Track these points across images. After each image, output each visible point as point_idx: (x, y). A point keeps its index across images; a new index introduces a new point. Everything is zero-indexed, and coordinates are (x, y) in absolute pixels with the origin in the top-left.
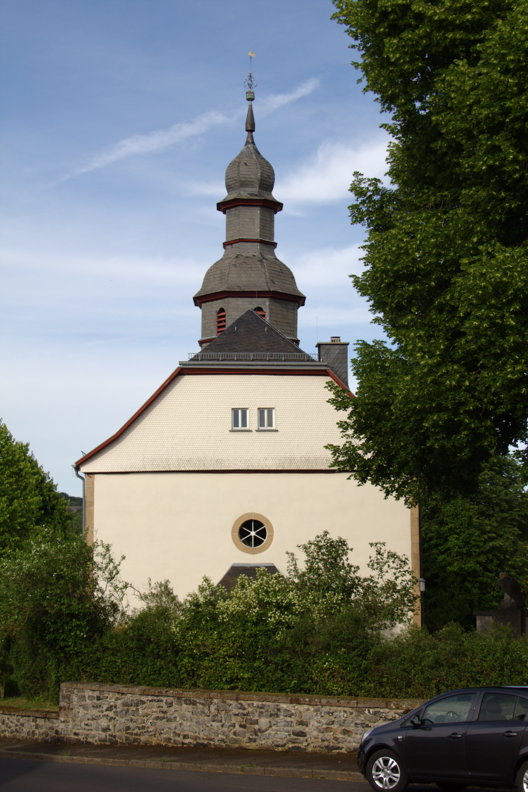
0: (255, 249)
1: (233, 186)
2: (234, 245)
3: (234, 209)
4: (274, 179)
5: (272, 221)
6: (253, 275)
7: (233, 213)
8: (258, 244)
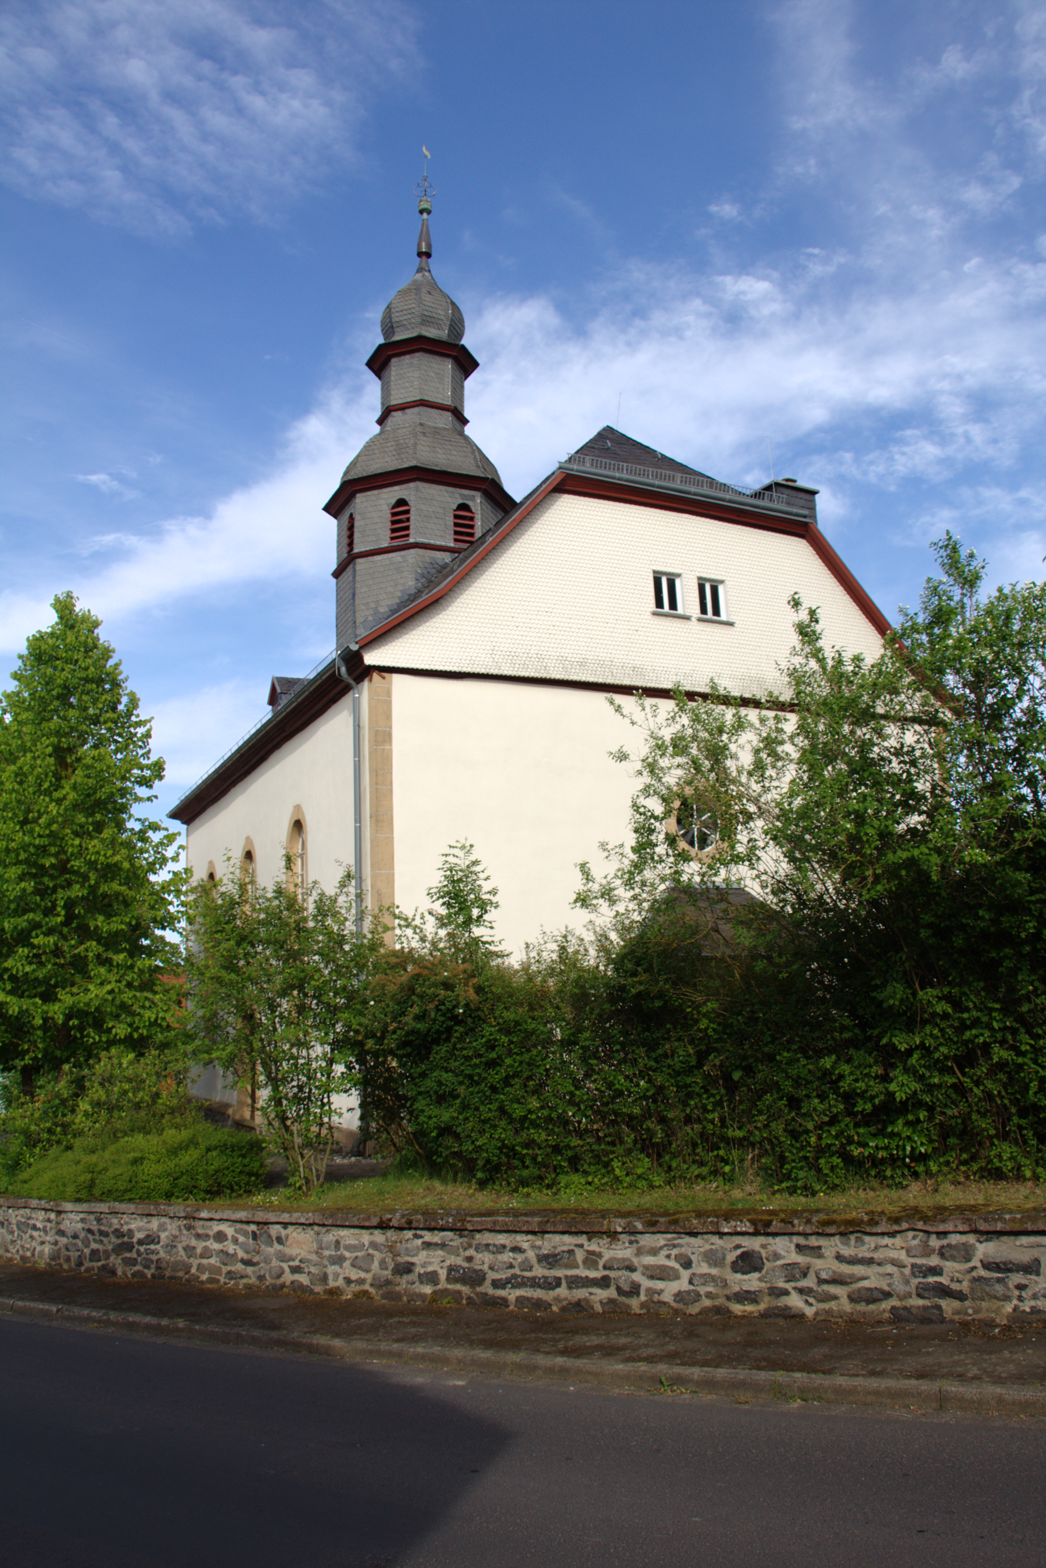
0: (446, 419)
1: (405, 323)
2: (407, 411)
3: (407, 357)
4: (464, 327)
5: (462, 387)
6: (454, 453)
7: (407, 361)
8: (449, 414)
